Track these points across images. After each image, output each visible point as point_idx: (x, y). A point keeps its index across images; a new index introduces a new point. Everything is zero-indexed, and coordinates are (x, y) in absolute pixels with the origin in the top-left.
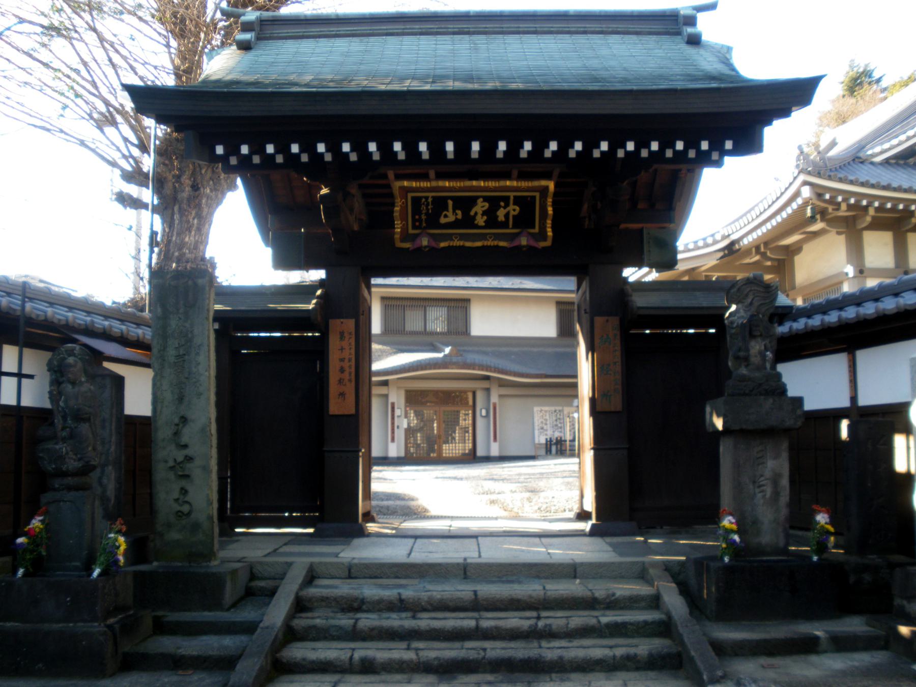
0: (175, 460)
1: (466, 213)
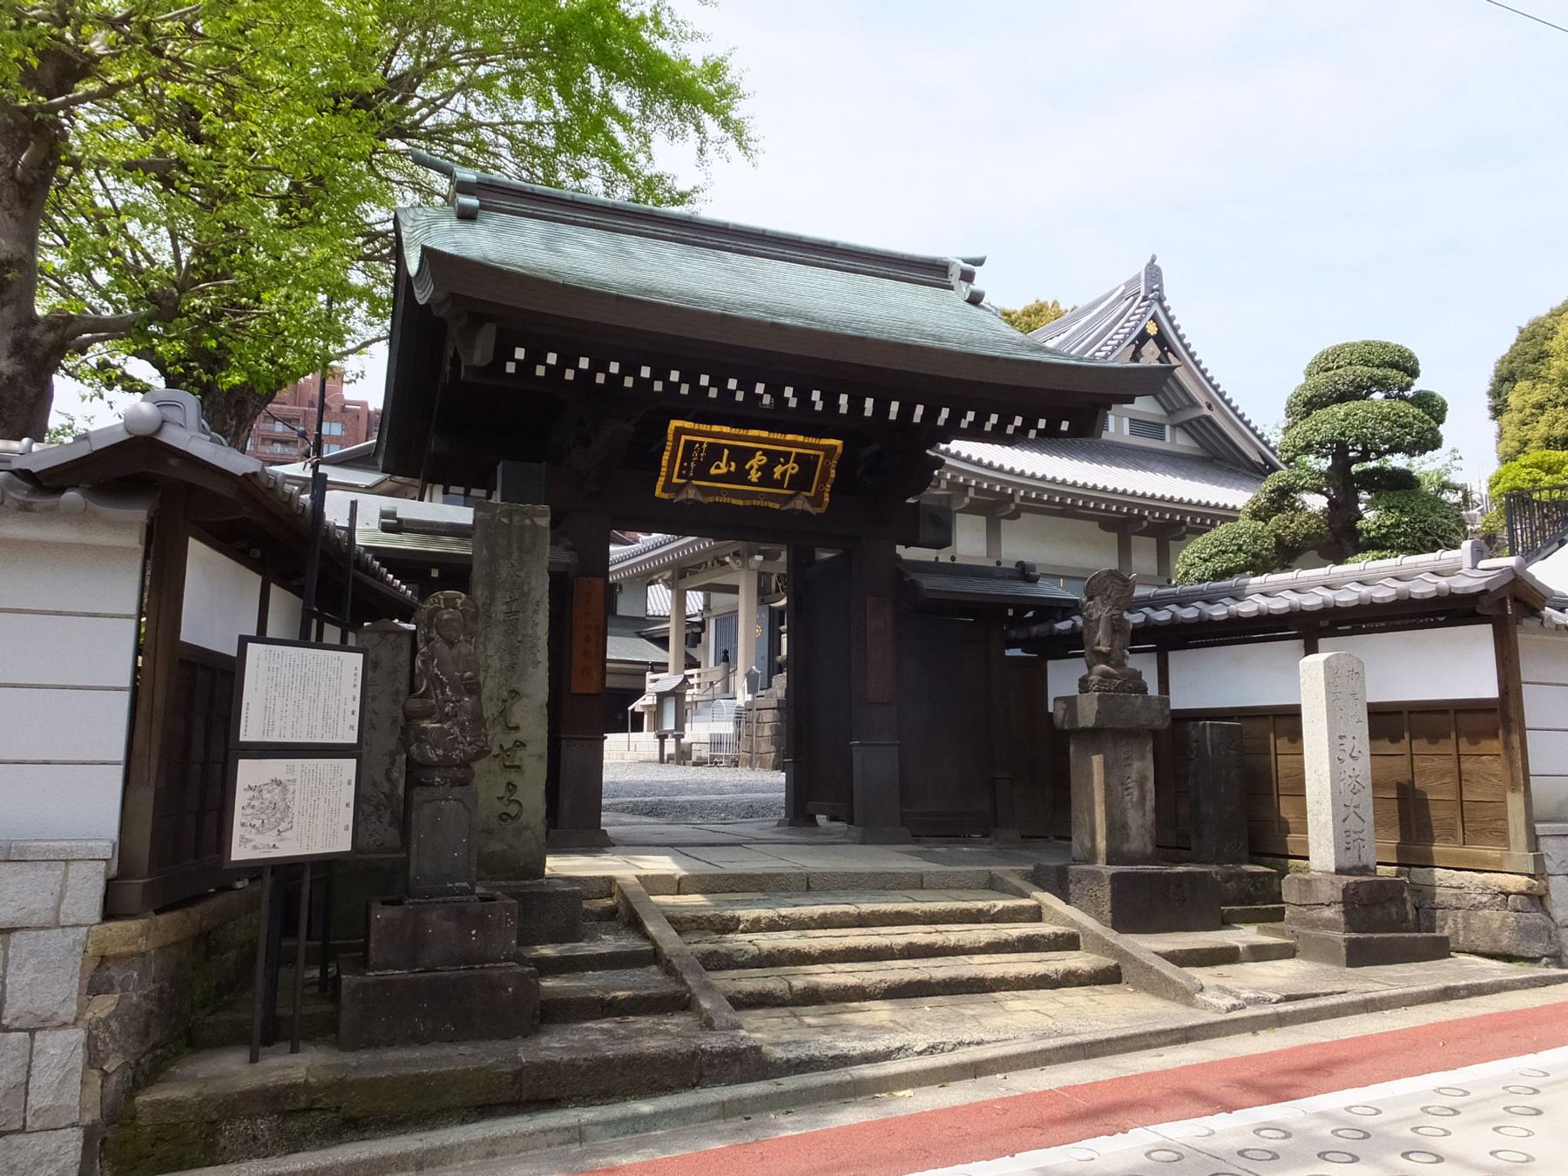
1: (740, 466)
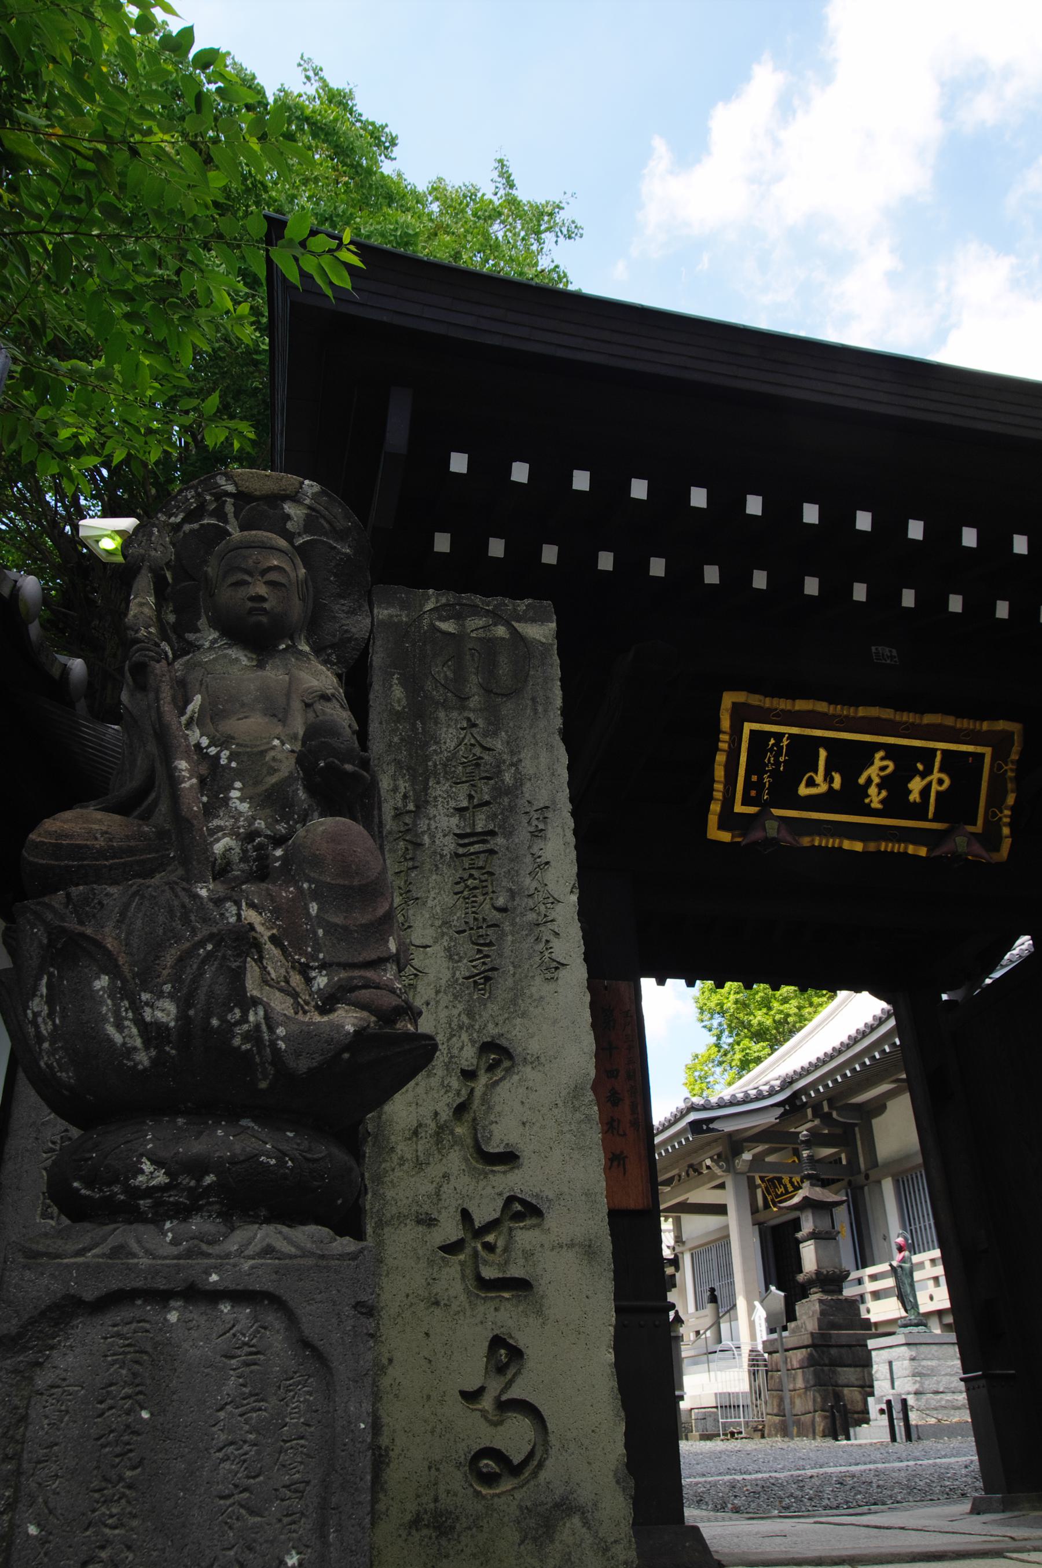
0: (466, 1216)
1: (850, 780)
